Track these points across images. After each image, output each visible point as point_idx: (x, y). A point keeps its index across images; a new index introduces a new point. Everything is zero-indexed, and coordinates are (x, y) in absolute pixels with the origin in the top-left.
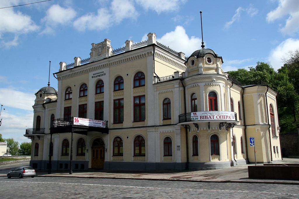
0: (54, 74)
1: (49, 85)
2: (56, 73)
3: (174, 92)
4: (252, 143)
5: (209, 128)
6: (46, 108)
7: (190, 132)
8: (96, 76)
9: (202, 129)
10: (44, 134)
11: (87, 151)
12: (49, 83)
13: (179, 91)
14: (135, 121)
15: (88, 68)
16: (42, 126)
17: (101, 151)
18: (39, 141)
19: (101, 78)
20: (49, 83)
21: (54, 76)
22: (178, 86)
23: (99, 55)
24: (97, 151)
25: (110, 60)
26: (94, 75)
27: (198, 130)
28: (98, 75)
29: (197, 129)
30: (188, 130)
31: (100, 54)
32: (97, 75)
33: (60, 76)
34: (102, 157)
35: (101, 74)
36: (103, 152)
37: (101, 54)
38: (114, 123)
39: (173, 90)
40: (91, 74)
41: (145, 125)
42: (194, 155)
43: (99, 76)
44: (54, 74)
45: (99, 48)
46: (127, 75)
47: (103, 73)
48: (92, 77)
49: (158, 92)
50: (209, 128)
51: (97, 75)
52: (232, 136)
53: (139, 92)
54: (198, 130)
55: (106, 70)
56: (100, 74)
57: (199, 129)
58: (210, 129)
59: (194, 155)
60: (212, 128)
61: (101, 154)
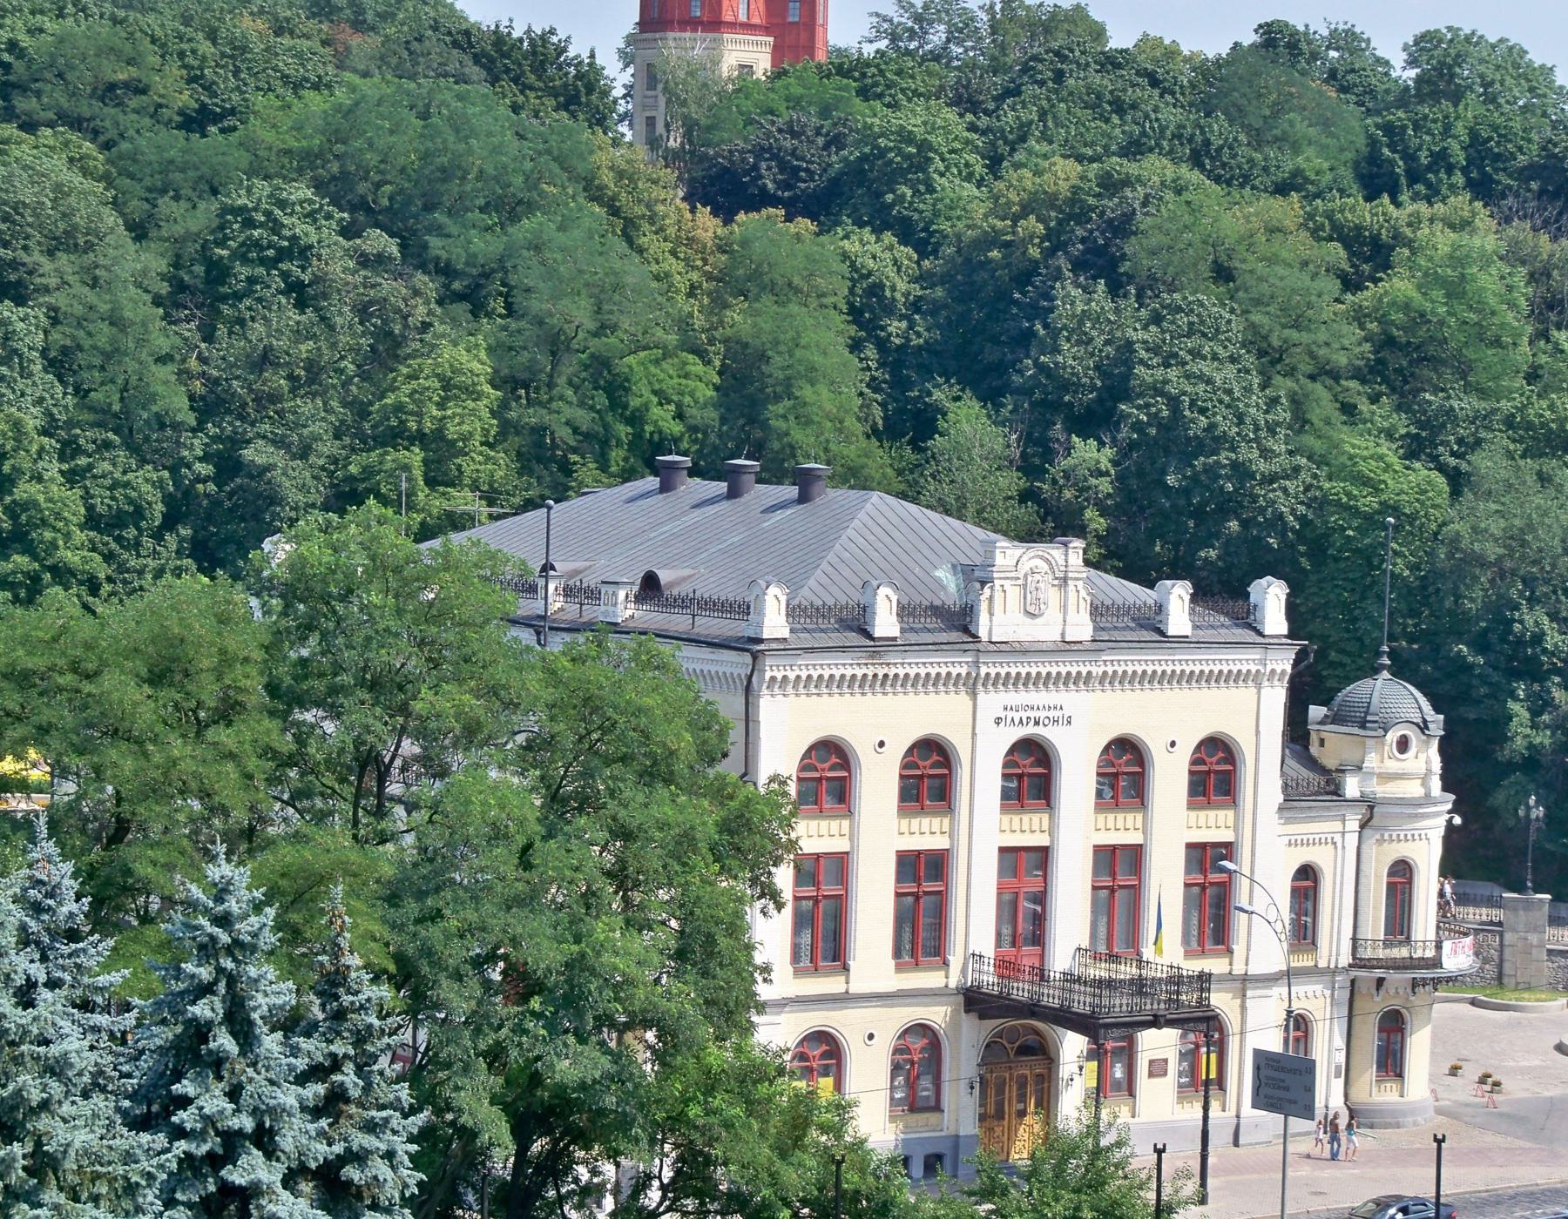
3: (1339, 845)
8: (1017, 721)
15: (983, 670)
19: (1050, 733)
26: (1010, 714)
28: (1032, 714)
32: (1024, 715)
35: (1051, 714)
39: (1338, 838)
40: (992, 702)
41: (1238, 969)
43: (1037, 723)
45: (1037, 577)
46: (1173, 744)
47: (1057, 714)
48: (998, 721)
51: (1024, 715)
53: (1213, 826)
56: (1042, 714)
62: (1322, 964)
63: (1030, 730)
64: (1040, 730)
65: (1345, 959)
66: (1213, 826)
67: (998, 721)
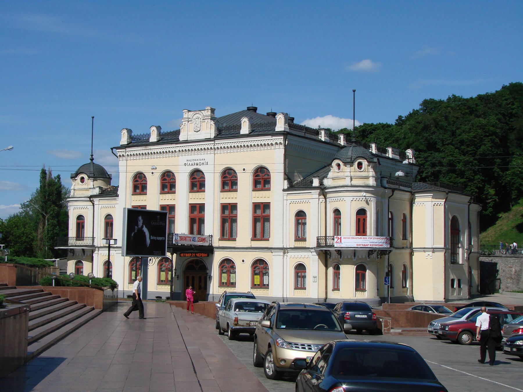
0: (112, 149)
1: (92, 160)
2: (115, 148)
4: (387, 282)
5: (355, 256)
6: (96, 203)
7: (331, 260)
8: (192, 165)
9: (346, 257)
10: (93, 246)
11: (178, 277)
12: (92, 156)
13: (319, 204)
14: (254, 238)
16: (88, 232)
17: (200, 278)
18: (84, 257)
20: (92, 156)
21: (113, 152)
22: (317, 196)
23: (197, 132)
24: (193, 278)
25: (216, 143)
26: (189, 162)
27: (340, 258)
28: (195, 162)
29: (339, 256)
30: (328, 256)
31: (199, 129)
32: (193, 162)
33: (124, 154)
34: (203, 286)
35: (201, 162)
36: (203, 281)
37: (200, 130)
38: (223, 238)
40: (183, 159)
41: (270, 246)
42: (334, 290)
43: (197, 165)
44: (112, 149)
45: (197, 120)
47: (204, 161)
48: (185, 164)
49: (289, 202)
50: (355, 256)
52: (386, 264)
53: (261, 197)
54: (340, 258)
55: (208, 157)
56: (198, 162)
57: (342, 256)
58: (356, 257)
59: (334, 290)
60: (358, 256)
61: (200, 281)
62: (307, 246)
63: (196, 167)
64: (198, 167)
65: (315, 245)
66: (261, 197)
67: (185, 164)
